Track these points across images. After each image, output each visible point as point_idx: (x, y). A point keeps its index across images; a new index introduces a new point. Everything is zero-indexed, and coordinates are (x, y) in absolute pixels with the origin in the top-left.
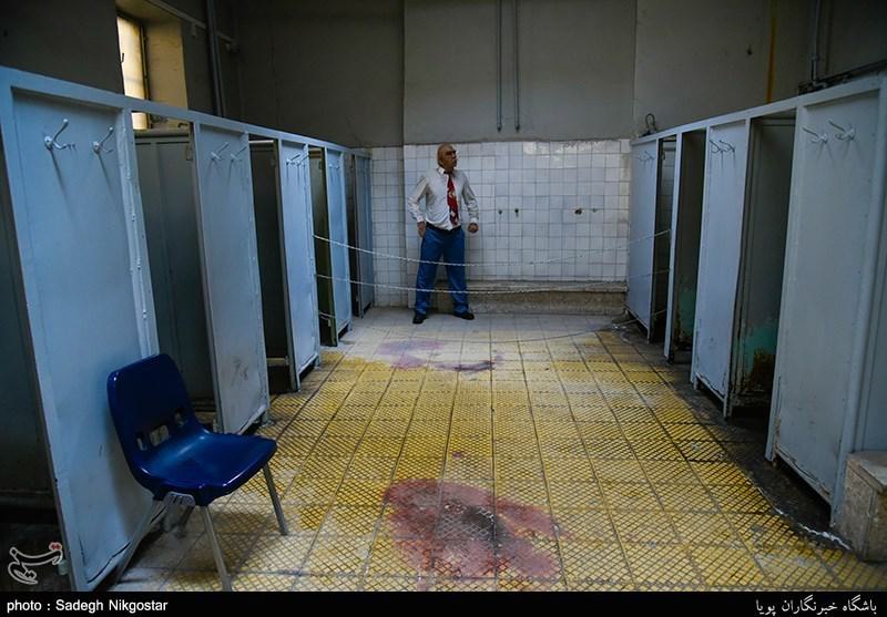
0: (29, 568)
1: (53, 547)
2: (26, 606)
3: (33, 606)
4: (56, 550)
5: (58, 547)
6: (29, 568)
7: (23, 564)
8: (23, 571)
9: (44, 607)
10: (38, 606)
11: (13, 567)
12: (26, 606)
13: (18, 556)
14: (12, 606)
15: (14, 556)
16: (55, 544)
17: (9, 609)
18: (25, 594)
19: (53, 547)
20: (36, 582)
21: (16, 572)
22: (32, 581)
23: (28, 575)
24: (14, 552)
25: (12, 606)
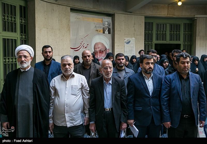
0: (7, 133)
1: (12, 128)
2: (7, 141)
3: (9, 141)
4: (13, 128)
5: (13, 128)
6: (7, 133)
7: (4, 131)
8: (5, 133)
9: (11, 141)
10: (10, 141)
11: (3, 132)
12: (7, 141)
13: (4, 130)
14: (4, 141)
15: (3, 130)
16: (13, 127)
17: (3, 142)
18: (6, 138)
19: (12, 128)
20: (8, 136)
21: (3, 133)
22: (7, 136)
23: (6, 134)
24: (3, 129)
25: (4, 141)
